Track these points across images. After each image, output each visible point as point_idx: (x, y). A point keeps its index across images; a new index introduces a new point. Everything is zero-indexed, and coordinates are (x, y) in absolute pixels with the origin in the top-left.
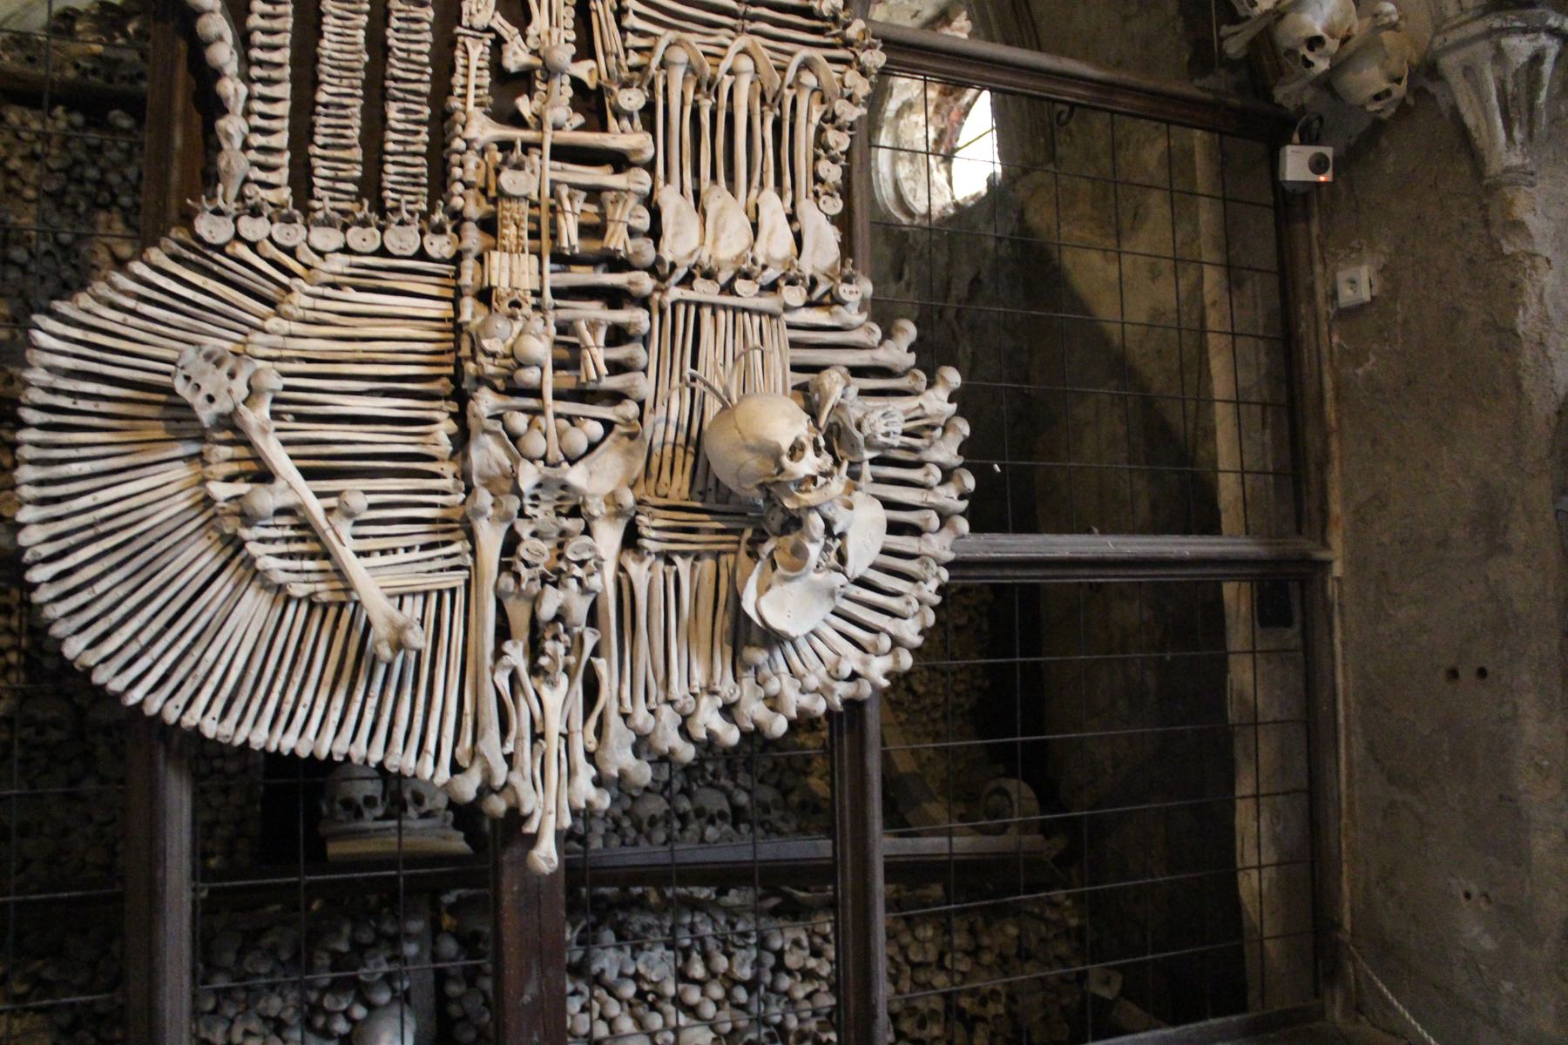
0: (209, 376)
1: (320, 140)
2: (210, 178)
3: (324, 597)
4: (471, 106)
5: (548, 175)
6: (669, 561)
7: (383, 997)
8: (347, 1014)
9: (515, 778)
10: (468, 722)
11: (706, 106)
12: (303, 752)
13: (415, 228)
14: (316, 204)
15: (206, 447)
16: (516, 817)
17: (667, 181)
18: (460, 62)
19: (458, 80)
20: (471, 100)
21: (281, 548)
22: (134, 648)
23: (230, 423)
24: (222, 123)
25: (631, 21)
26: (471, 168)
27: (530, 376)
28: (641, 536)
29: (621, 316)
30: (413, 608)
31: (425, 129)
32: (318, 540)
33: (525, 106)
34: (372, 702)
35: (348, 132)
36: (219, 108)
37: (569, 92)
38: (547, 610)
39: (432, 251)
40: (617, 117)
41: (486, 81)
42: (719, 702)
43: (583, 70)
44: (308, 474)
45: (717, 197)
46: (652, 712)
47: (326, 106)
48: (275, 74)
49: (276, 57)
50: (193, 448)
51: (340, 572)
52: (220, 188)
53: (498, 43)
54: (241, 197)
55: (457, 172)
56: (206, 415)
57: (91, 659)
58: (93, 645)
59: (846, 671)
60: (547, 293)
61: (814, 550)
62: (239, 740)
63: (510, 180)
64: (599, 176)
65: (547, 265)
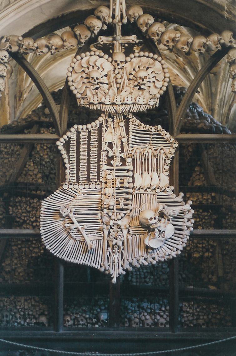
2: (64, 180)
3: (81, 240)
4: (103, 164)
6: (135, 236)
7: (103, 308)
8: (96, 310)
9: (109, 268)
10: (103, 260)
11: (143, 158)
12: (78, 263)
13: (95, 184)
14: (80, 182)
15: (65, 219)
18: (101, 156)
19: (101, 159)
20: (103, 162)
21: (75, 233)
22: (55, 247)
23: (67, 216)
25: (130, 145)
26: (103, 174)
30: (95, 242)
32: (80, 232)
33: (112, 162)
34: (89, 256)
36: (66, 168)
37: (120, 159)
38: (114, 243)
40: (128, 162)
41: (106, 159)
42: (144, 258)
43: (122, 155)
44: (79, 223)
45: (145, 174)
46: (132, 259)
49: (74, 159)
50: (63, 219)
51: (83, 237)
52: (66, 181)
53: (108, 152)
54: (69, 182)
55: (101, 175)
56: (64, 215)
57: (50, 249)
59: (167, 254)
60: (115, 193)
61: (157, 235)
62: (69, 261)
63: (108, 177)
65: (115, 189)
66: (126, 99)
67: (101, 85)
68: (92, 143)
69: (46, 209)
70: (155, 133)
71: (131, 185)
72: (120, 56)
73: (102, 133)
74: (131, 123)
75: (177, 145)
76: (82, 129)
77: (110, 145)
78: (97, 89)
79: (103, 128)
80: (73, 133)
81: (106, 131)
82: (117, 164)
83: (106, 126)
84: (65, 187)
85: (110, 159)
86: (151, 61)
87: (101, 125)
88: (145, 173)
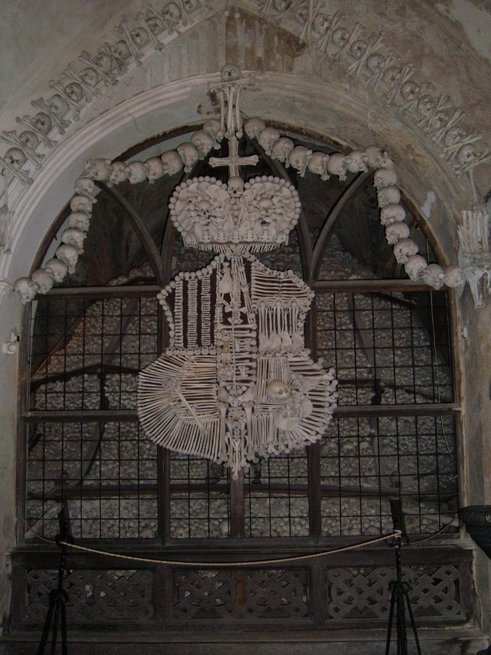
2: (168, 344)
4: (218, 322)
10: (220, 448)
16: (229, 469)
25: (253, 297)
26: (218, 336)
29: (250, 364)
33: (230, 320)
36: (170, 329)
37: (240, 315)
41: (222, 315)
44: (187, 400)
45: (273, 334)
53: (224, 306)
54: (174, 346)
64: (247, 334)
66: (245, 237)
67: (212, 219)
69: (145, 383)
70: (285, 280)
71: (254, 349)
72: (235, 183)
74: (253, 268)
76: (190, 278)
77: (227, 297)
78: (207, 224)
79: (217, 276)
81: (221, 278)
83: (221, 272)
84: (169, 353)
85: (226, 315)
86: (277, 187)
87: (215, 271)
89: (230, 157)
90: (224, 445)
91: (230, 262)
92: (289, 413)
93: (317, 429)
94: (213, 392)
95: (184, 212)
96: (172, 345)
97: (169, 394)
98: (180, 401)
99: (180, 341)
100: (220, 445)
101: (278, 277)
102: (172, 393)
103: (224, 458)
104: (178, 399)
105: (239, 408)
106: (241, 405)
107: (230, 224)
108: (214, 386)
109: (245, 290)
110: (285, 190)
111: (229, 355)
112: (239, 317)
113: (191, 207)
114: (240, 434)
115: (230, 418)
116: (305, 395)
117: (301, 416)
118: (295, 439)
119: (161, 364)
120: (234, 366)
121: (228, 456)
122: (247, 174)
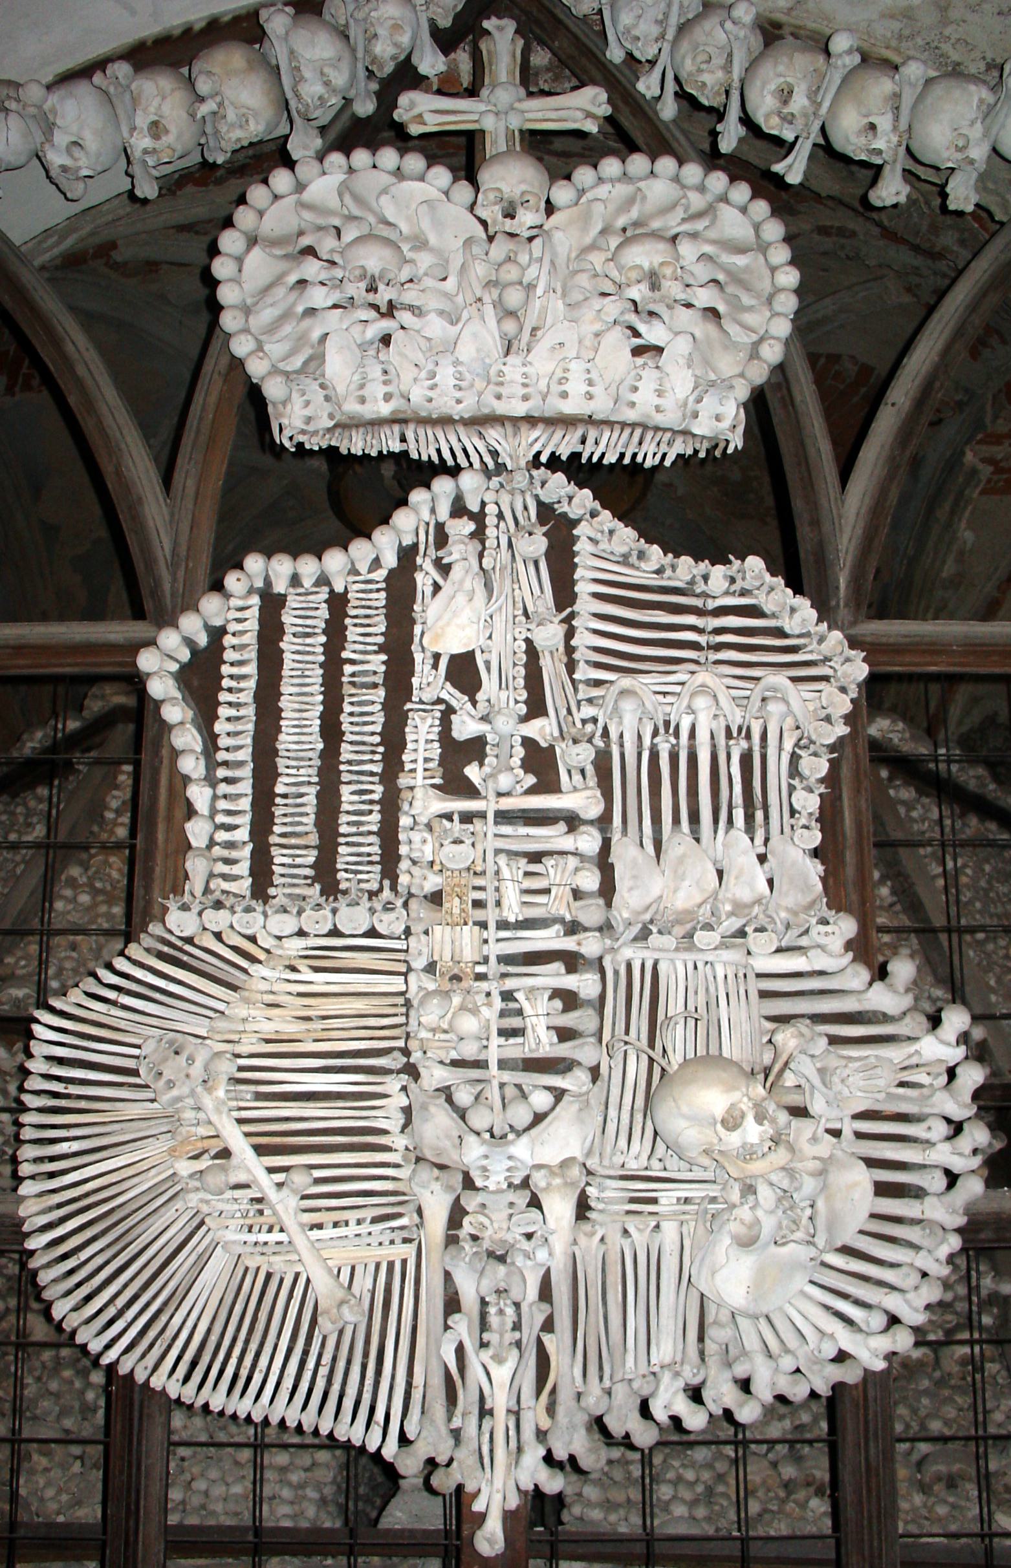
0: (169, 1063)
1: (277, 829)
4: (419, 781)
5: (492, 844)
10: (417, 1395)
14: (272, 891)
17: (625, 831)
18: (409, 738)
20: (420, 773)
22: (111, 1311)
24: (189, 826)
25: (583, 672)
26: (415, 844)
27: (469, 1051)
28: (590, 1208)
29: (571, 982)
31: (377, 808)
33: (472, 772)
35: (304, 820)
37: (520, 752)
39: (381, 929)
41: (436, 751)
42: (681, 1384)
44: (260, 1150)
45: (678, 843)
47: (285, 796)
48: (237, 773)
53: (449, 711)
54: (207, 891)
55: (403, 850)
58: (75, 1309)
60: (493, 960)
64: (553, 837)
67: (405, 317)
68: (353, 662)
69: (61, 1061)
73: (414, 601)
74: (582, 547)
75: (861, 671)
76: (295, 581)
77: (464, 672)
79: (419, 577)
80: (240, 603)
81: (437, 588)
82: (505, 781)
83: (437, 563)
84: (179, 922)
85: (458, 755)
87: (408, 555)
88: (677, 838)
89: (484, 92)
90: (437, 1382)
91: (479, 518)
92: (768, 1224)
93: (893, 1302)
94: (387, 1116)
95: (280, 292)
96: (196, 884)
97: (173, 1118)
98: (225, 1154)
99: (235, 870)
100: (418, 1380)
101: (700, 587)
102: (189, 1115)
103: (432, 1441)
104: (215, 1146)
105: (511, 1196)
106: (525, 1183)
107: (480, 336)
108: (393, 1085)
109: (549, 636)
110: (728, 214)
111: (468, 936)
112: (516, 762)
113: (311, 269)
114: (517, 1327)
115: (468, 1246)
116: (836, 1133)
117: (820, 1241)
118: (787, 1351)
119: (139, 973)
120: (494, 987)
121: (456, 1434)
122: (557, 152)
